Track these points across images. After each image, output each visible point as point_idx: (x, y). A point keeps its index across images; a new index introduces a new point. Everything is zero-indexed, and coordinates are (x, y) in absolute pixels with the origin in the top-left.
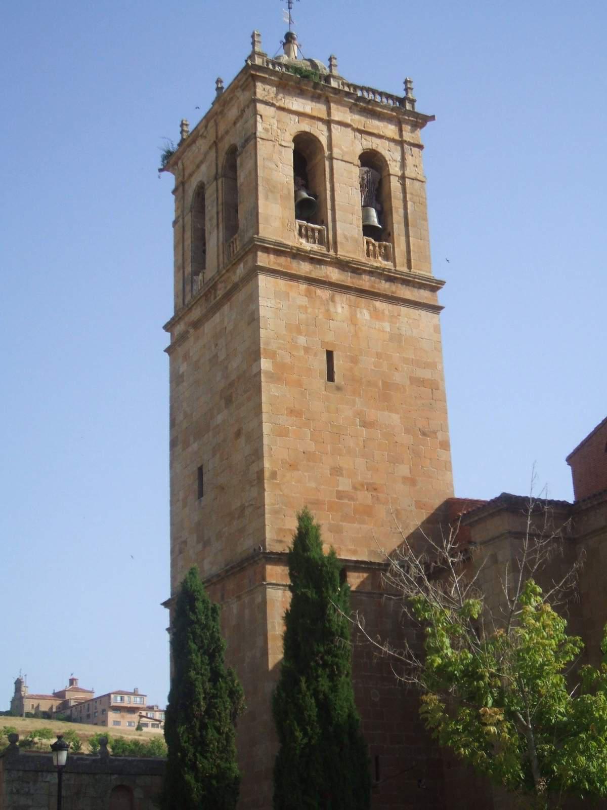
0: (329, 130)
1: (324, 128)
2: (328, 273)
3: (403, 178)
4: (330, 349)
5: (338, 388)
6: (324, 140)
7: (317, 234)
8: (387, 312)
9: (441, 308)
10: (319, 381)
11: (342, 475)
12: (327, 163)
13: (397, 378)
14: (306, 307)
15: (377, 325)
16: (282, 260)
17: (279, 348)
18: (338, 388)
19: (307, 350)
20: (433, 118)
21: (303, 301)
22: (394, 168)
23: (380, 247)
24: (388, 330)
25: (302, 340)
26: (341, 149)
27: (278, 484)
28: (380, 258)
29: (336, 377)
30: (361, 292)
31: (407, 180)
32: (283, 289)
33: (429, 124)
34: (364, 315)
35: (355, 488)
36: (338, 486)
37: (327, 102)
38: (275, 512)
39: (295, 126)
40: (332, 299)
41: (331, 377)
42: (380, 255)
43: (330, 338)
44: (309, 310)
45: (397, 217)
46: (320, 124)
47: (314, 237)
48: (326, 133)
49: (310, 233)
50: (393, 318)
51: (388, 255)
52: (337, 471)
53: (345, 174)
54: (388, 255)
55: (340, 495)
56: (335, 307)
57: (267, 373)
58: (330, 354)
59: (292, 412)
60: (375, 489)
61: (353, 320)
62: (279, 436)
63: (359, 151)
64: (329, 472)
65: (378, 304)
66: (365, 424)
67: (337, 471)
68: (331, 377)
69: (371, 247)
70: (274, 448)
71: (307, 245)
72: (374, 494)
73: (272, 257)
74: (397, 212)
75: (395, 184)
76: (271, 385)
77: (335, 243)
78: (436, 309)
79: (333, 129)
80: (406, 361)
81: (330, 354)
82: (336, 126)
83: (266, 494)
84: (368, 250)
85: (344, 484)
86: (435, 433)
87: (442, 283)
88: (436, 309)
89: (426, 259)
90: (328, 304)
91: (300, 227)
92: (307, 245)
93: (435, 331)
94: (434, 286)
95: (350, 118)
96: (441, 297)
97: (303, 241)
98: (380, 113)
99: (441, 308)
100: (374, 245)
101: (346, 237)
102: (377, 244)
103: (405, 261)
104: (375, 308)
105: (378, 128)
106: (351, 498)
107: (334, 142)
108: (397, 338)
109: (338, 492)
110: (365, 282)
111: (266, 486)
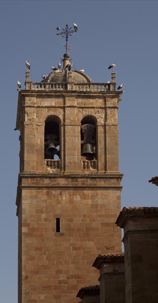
0: (64, 111)
1: (62, 110)
2: (59, 182)
3: (105, 126)
4: (58, 217)
5: (62, 235)
6: (61, 117)
7: (56, 164)
8: (90, 195)
9: (121, 187)
10: (52, 232)
11: (61, 273)
12: (62, 128)
13: (94, 225)
14: (46, 201)
15: (84, 202)
16: (35, 181)
17: (31, 221)
18: (62, 235)
19: (46, 220)
20: (150, 181)
21: (45, 198)
22: (100, 121)
23: (91, 162)
24: (91, 203)
25: (44, 216)
26: (70, 119)
27: (29, 281)
28: (91, 168)
29: (60, 230)
30: (76, 188)
31: (107, 127)
32: (35, 194)
33: (150, 179)
34: (77, 198)
35: (68, 278)
36: (59, 278)
37: (64, 97)
38: (27, 293)
39: (46, 114)
40: (61, 194)
41: (58, 230)
42: (91, 166)
43: (58, 212)
44: (48, 201)
45: (101, 146)
46: (59, 109)
47: (55, 165)
48: (62, 113)
49: (53, 164)
50: (93, 197)
51: (95, 166)
52: (59, 272)
53: (72, 131)
54: (95, 166)
55: (60, 282)
56: (62, 197)
57: (24, 233)
58: (58, 220)
59: (37, 249)
60: (79, 277)
61: (71, 201)
62: (31, 260)
63: (81, 117)
64: (55, 273)
65: (86, 192)
66: (75, 249)
67: (59, 272)
68: (58, 230)
69: (86, 164)
70: (27, 266)
71: (51, 170)
72: (78, 279)
73: (29, 180)
74: (100, 143)
75: (100, 130)
76: (27, 238)
77: (65, 166)
78: (120, 188)
79: (66, 111)
80: (100, 216)
81: (58, 220)
82: (67, 109)
83: (23, 286)
84: (84, 165)
85: (62, 277)
86: (113, 247)
87: (122, 175)
88: (120, 188)
89: (116, 164)
90: (58, 196)
91: (47, 162)
92: (51, 170)
93: (117, 199)
94: (119, 177)
95: (76, 102)
96: (122, 183)
97: (49, 168)
98: (93, 96)
99: (121, 187)
100: (87, 162)
101: (70, 163)
102: (89, 161)
103: (104, 167)
104: (84, 194)
105: (92, 103)
106: (66, 283)
107: (66, 117)
108: (95, 206)
109: (59, 281)
110: (80, 182)
111: (23, 283)
